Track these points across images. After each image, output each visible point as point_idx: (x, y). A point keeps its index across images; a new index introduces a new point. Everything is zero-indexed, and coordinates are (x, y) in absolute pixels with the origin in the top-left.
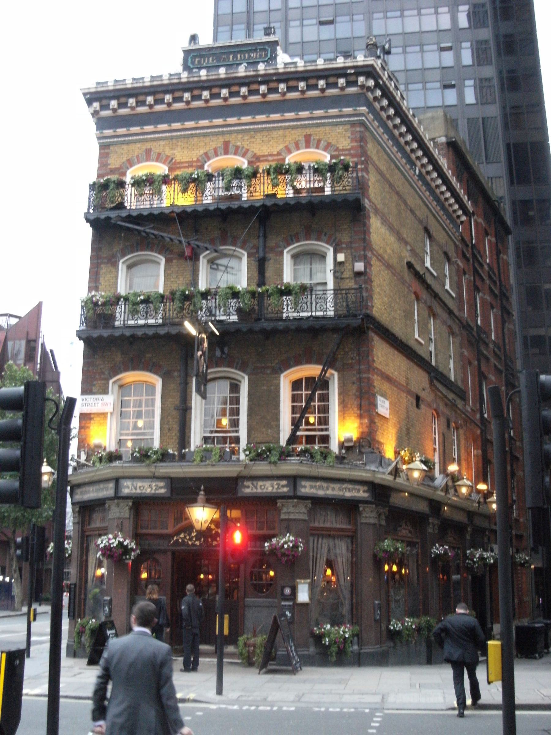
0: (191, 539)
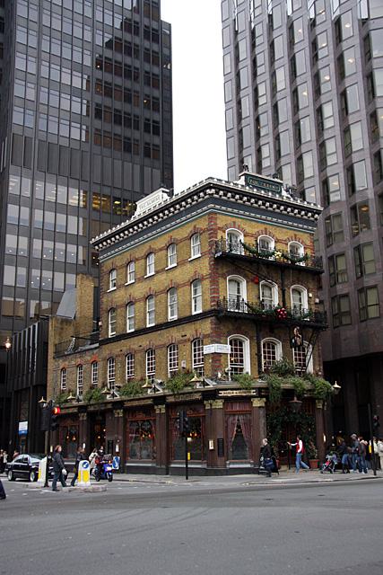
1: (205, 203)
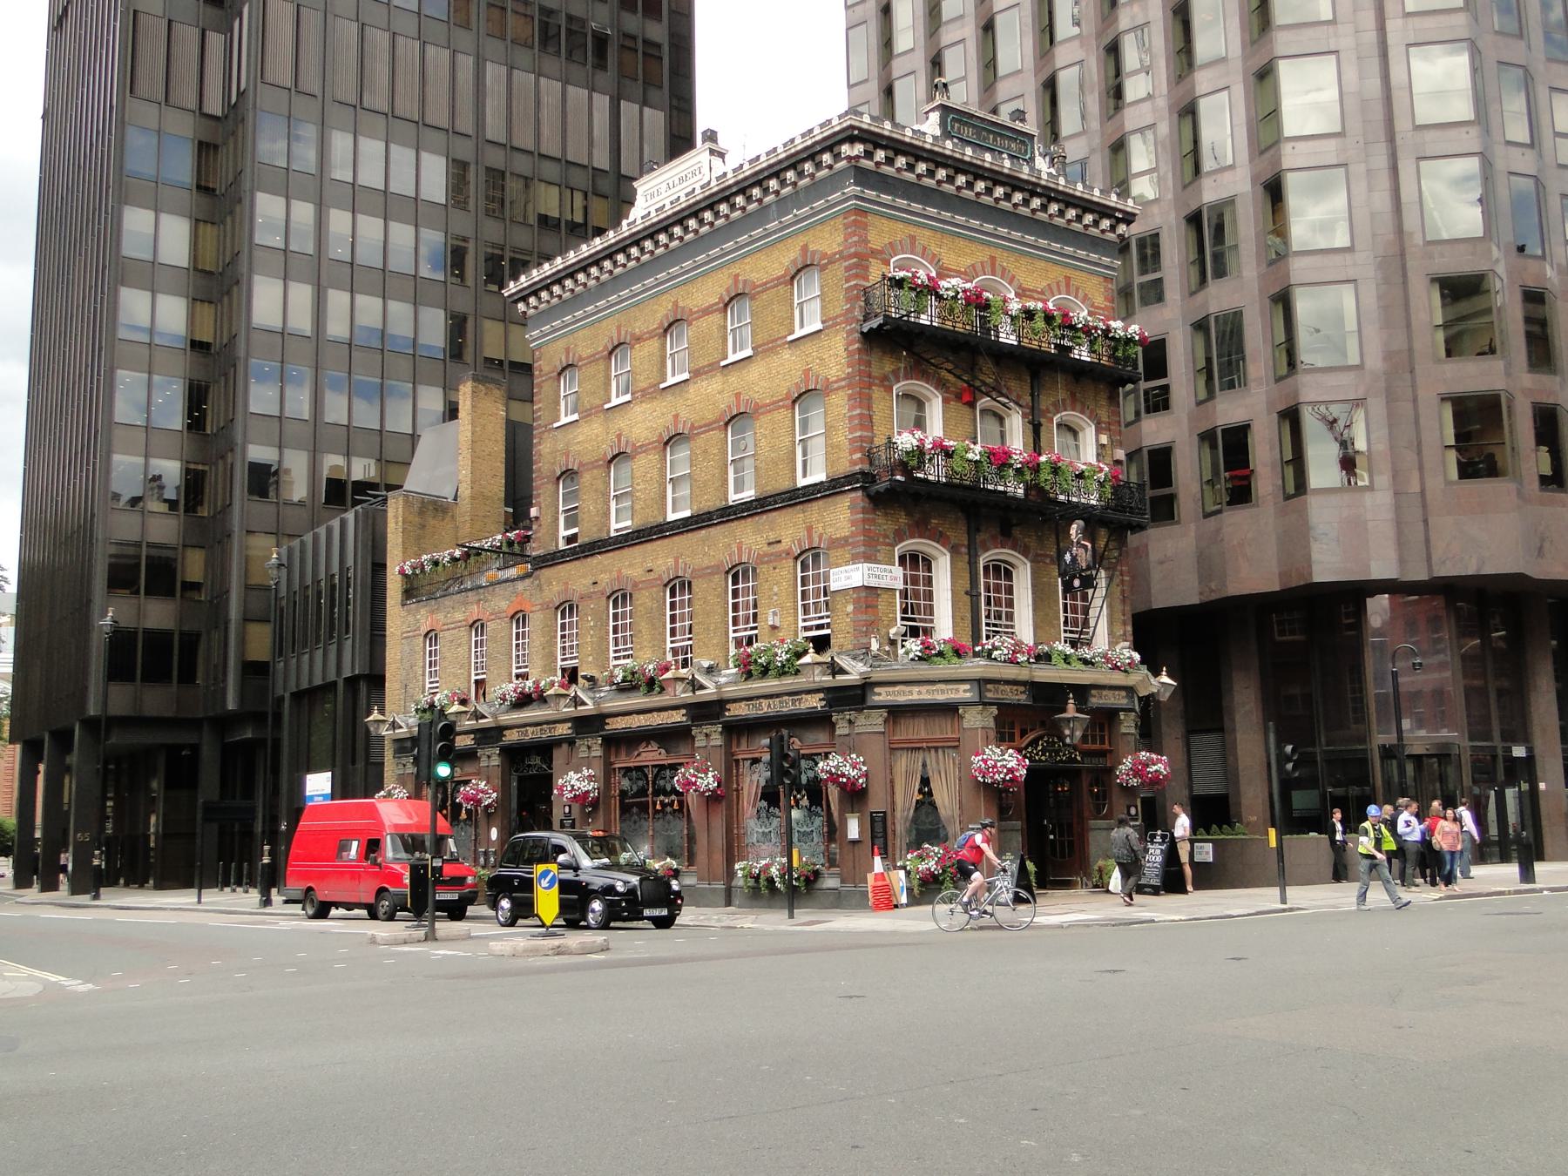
0: (1037, 754)
1: (835, 181)
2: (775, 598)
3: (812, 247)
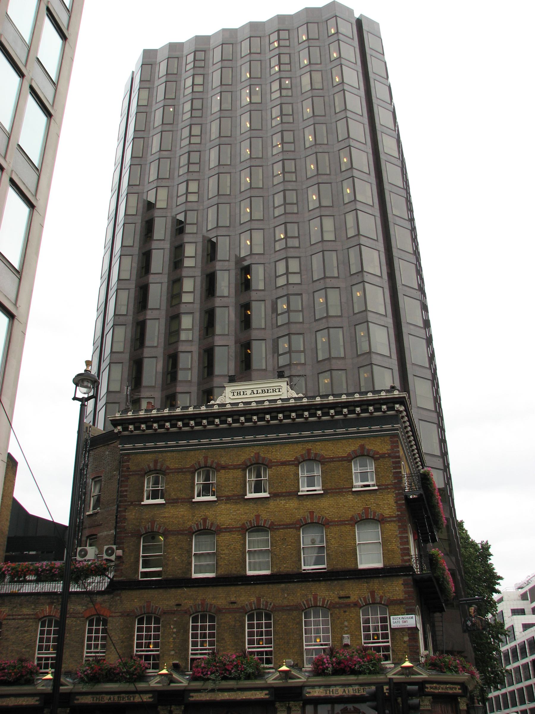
2: (346, 629)
3: (367, 447)
